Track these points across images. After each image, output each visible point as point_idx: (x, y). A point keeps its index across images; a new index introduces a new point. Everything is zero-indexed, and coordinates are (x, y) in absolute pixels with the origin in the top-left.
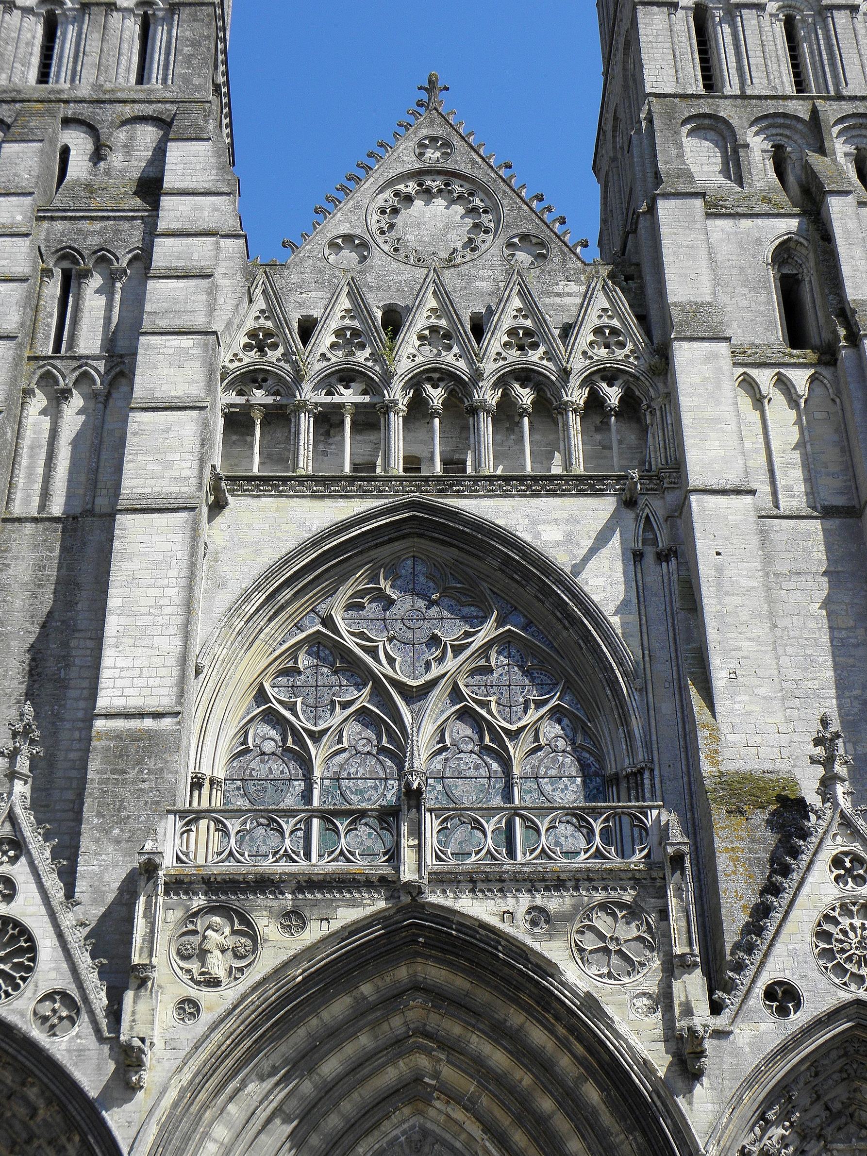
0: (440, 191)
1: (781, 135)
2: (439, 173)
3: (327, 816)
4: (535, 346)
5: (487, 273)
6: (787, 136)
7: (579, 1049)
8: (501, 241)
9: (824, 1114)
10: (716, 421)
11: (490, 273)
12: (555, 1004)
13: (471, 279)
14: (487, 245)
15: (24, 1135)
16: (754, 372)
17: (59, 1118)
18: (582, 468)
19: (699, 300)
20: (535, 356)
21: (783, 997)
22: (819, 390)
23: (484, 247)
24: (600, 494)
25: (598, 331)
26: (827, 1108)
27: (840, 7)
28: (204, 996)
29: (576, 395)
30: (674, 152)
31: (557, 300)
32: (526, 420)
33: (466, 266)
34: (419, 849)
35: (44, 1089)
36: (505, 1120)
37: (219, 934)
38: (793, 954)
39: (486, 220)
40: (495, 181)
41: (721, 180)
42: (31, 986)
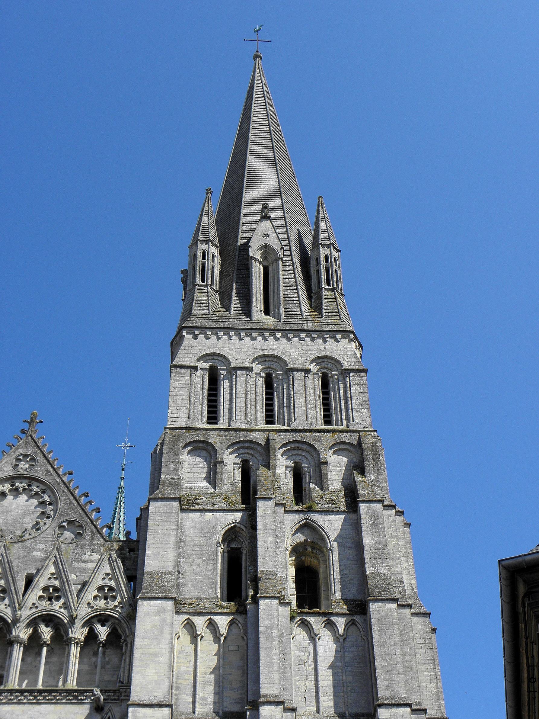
0: (24, 489)
1: (248, 453)
2: (25, 478)
4: (58, 598)
5: (41, 546)
6: (251, 454)
8: (55, 524)
10: (156, 655)
11: (44, 546)
13: (30, 550)
14: (46, 526)
16: (194, 618)
18: (75, 683)
19: (164, 570)
20: (57, 606)
22: (235, 630)
23: (44, 528)
24: (81, 702)
25: (101, 589)
27: (298, 370)
29: (78, 633)
30: (172, 467)
31: (83, 565)
32: (45, 649)
33: (29, 542)
39: (49, 509)
40: (59, 484)
41: (205, 484)
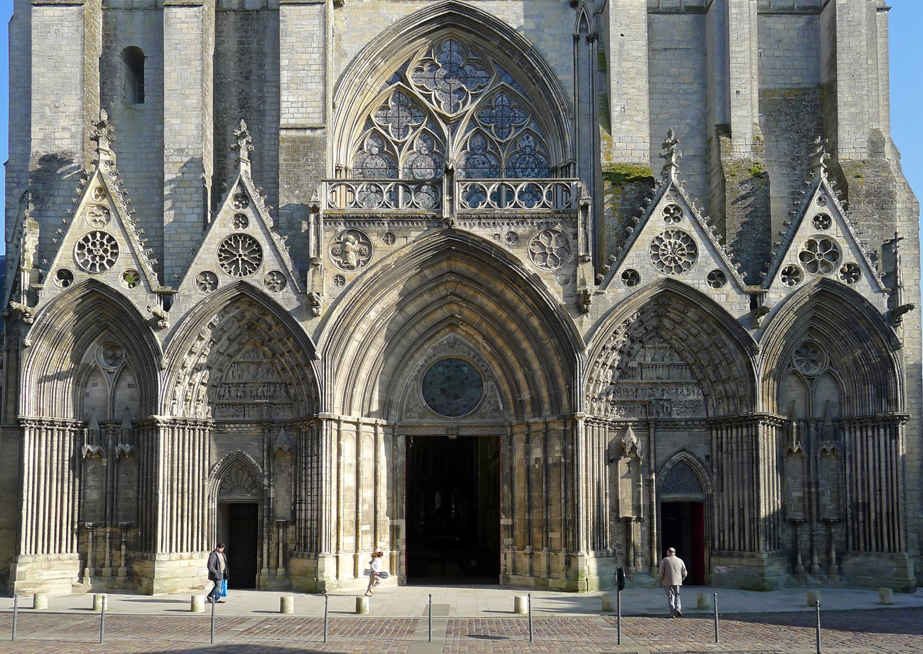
3: (406, 184)
7: (530, 301)
9: (644, 331)
12: (519, 279)
15: (267, 338)
17: (282, 330)
21: (631, 277)
26: (646, 329)
28: (349, 275)
34: (451, 201)
35: (274, 317)
36: (493, 334)
37: (353, 245)
38: (638, 256)
42: (261, 268)
